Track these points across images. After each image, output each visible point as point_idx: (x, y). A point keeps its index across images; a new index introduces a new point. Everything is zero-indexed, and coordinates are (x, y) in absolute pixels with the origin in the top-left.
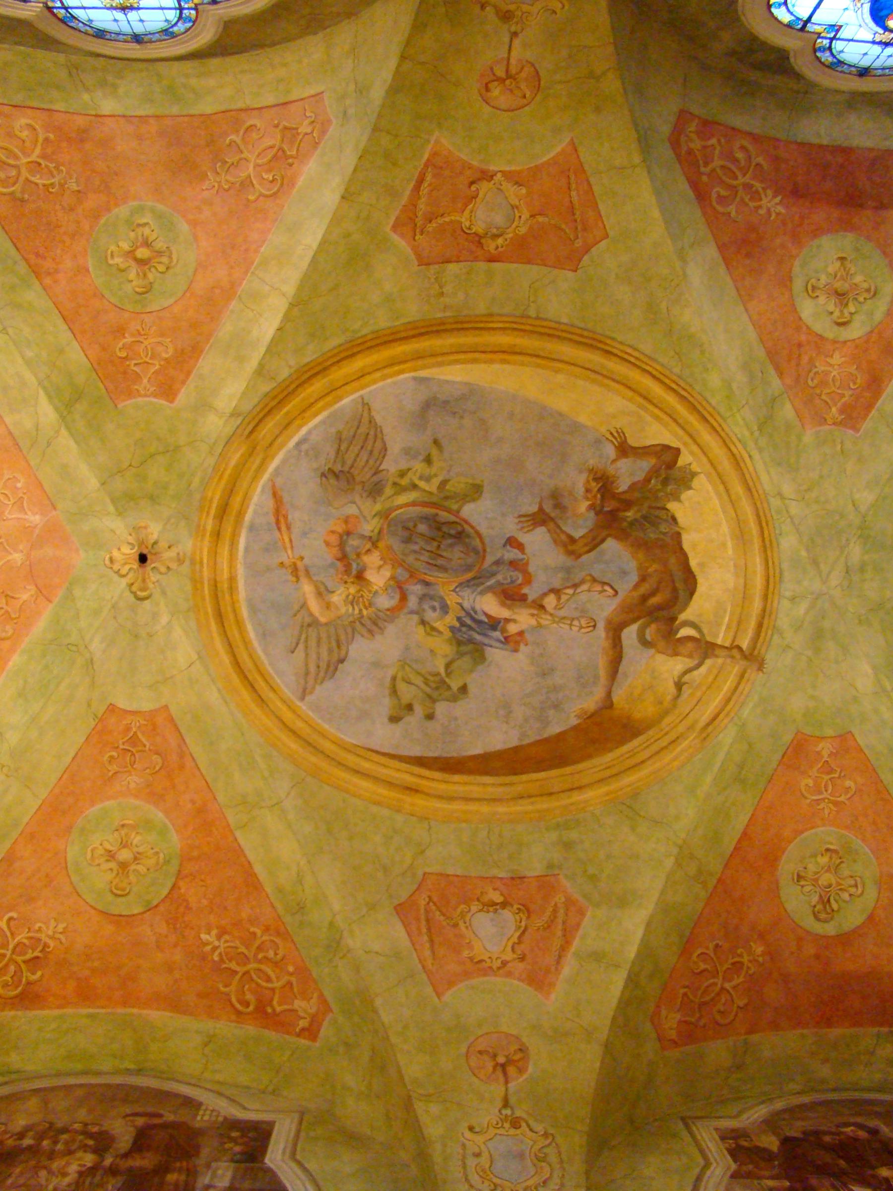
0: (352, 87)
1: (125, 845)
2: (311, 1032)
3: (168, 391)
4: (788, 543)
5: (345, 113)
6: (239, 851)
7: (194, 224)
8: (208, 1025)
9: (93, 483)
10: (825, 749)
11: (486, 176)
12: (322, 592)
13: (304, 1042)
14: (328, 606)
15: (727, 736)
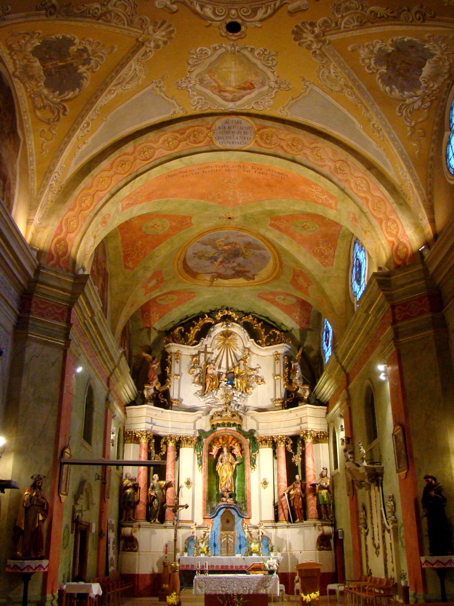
0: (330, 275)
1: (158, 226)
2: (126, 267)
3: (270, 225)
4: (234, 289)
5: (326, 272)
6: (161, 244)
7: (311, 235)
8: (120, 246)
9: (250, 212)
10: (193, 295)
11: (308, 285)
12: (222, 241)
13: (123, 266)
14: (219, 242)
15: (194, 287)
